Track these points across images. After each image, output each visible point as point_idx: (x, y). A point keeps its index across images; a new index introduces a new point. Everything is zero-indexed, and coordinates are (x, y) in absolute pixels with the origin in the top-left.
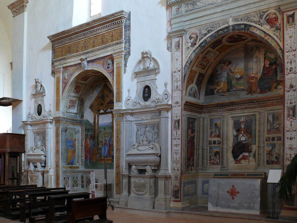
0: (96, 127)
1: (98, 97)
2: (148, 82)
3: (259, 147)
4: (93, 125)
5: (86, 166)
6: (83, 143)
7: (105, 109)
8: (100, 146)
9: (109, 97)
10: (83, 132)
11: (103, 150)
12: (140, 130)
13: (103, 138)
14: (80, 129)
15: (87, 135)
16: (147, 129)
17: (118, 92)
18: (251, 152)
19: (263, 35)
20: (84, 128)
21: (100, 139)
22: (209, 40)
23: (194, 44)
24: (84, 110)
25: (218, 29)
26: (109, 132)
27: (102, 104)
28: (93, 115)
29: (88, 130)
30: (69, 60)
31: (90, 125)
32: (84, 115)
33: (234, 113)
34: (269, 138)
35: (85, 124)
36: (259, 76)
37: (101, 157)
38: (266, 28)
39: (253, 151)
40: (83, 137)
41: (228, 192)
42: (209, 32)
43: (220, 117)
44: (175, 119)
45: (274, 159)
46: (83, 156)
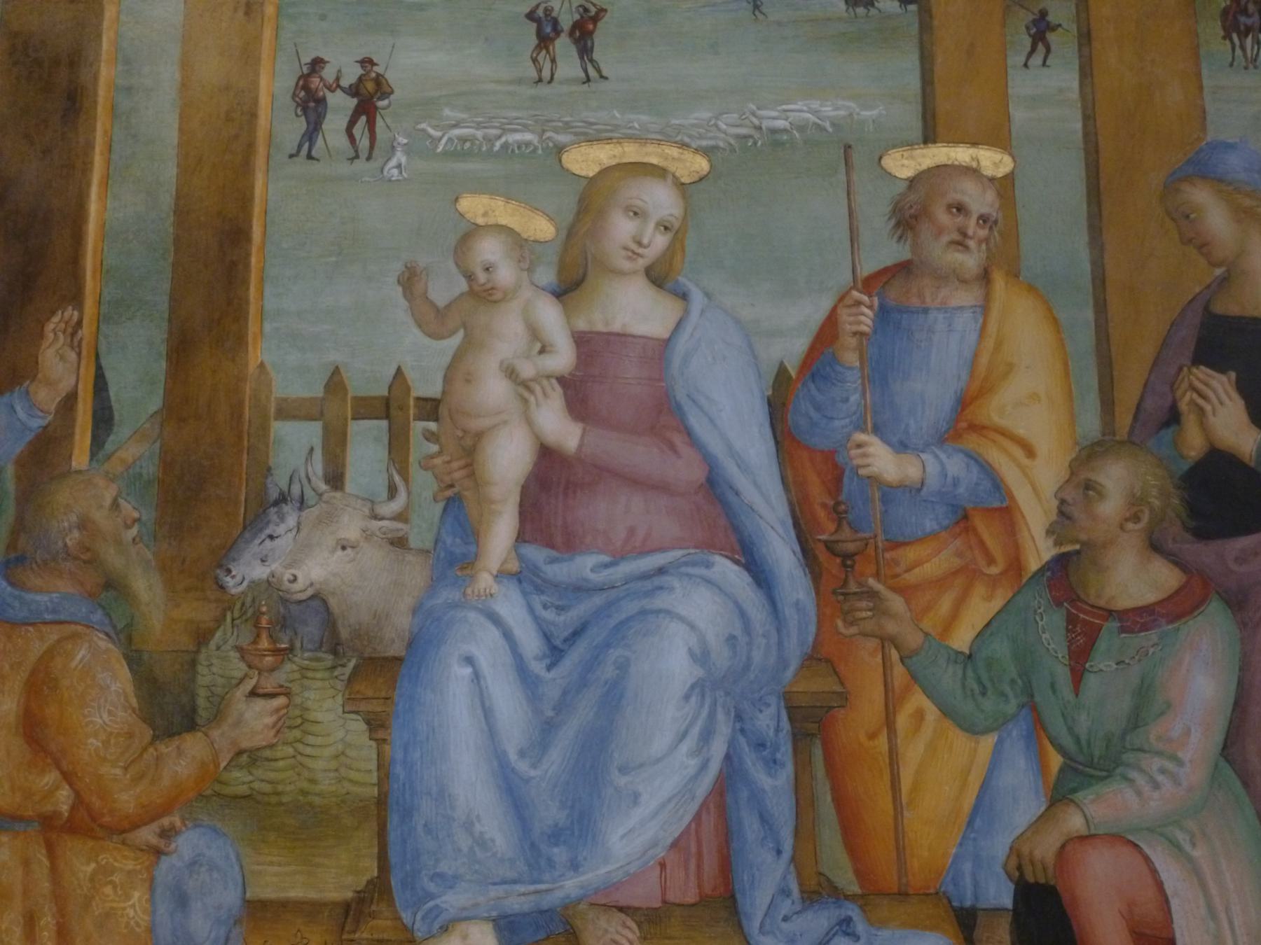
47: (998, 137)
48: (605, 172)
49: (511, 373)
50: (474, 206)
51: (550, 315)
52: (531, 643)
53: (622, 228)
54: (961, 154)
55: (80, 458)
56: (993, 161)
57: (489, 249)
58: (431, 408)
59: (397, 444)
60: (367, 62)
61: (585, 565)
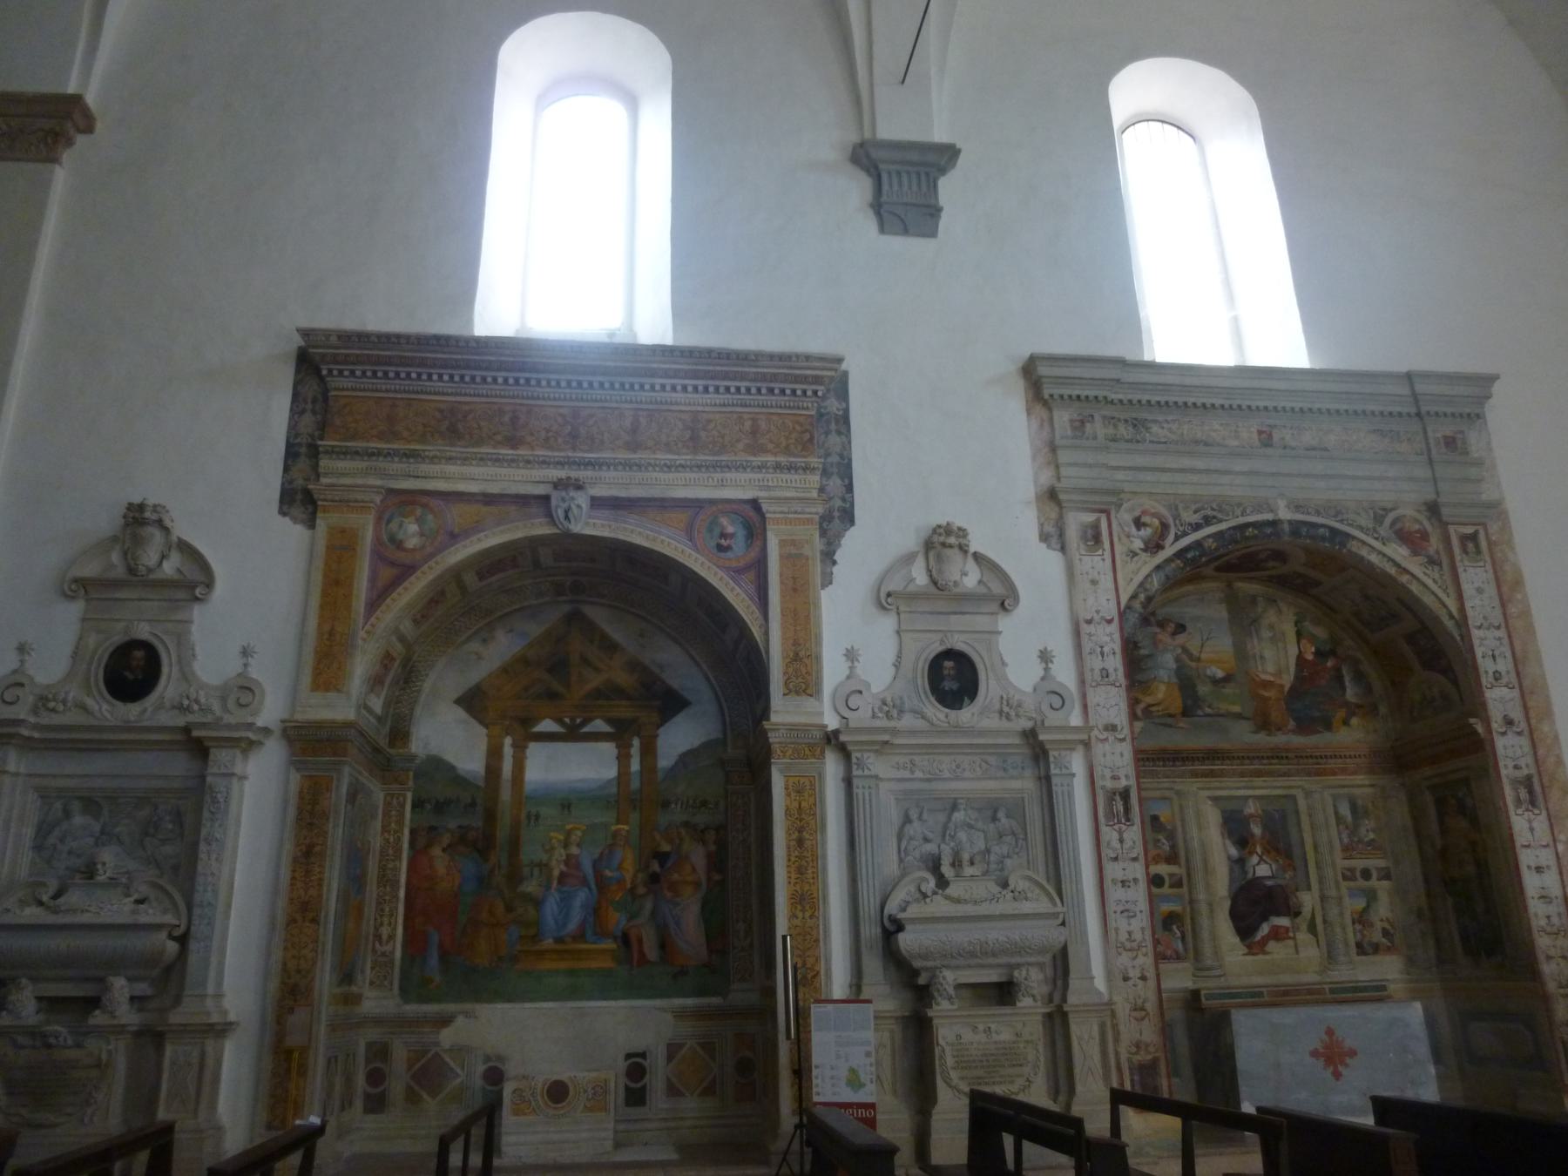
0: (506, 794)
1: (522, 662)
2: (963, 637)
3: (1323, 898)
4: (481, 783)
5: (413, 987)
6: (397, 870)
7: (572, 719)
8: (530, 887)
9: (597, 670)
10: (401, 815)
11: (551, 908)
12: (920, 818)
13: (553, 848)
14: (382, 795)
15: (432, 829)
16: (959, 816)
17: (797, 654)
18: (1297, 914)
19: (1392, 571)
20: (409, 796)
21: (530, 852)
22: (1210, 544)
23: (1154, 546)
24: (418, 711)
25: (1242, 520)
26: (596, 821)
27: (552, 696)
28: (486, 739)
29: (440, 807)
30: (452, 469)
31: (459, 780)
32: (414, 730)
33: (1217, 784)
34: (1352, 870)
35: (416, 777)
36: (1287, 680)
37: (536, 938)
38: (1399, 552)
39: (1306, 912)
40: (399, 839)
41: (1314, 1054)
42: (1208, 521)
43: (1167, 794)
44: (1109, 784)
45: (1377, 937)
46: (392, 937)
47: (627, 823)
48: (571, 829)
49: (557, 860)
50: (552, 834)
51: (562, 851)
52: (558, 899)
53: (574, 837)
54: (622, 826)
55: (496, 872)
56: (626, 827)
57: (554, 841)
58: (546, 865)
59: (541, 870)
60: (537, 812)
61: (565, 889)
